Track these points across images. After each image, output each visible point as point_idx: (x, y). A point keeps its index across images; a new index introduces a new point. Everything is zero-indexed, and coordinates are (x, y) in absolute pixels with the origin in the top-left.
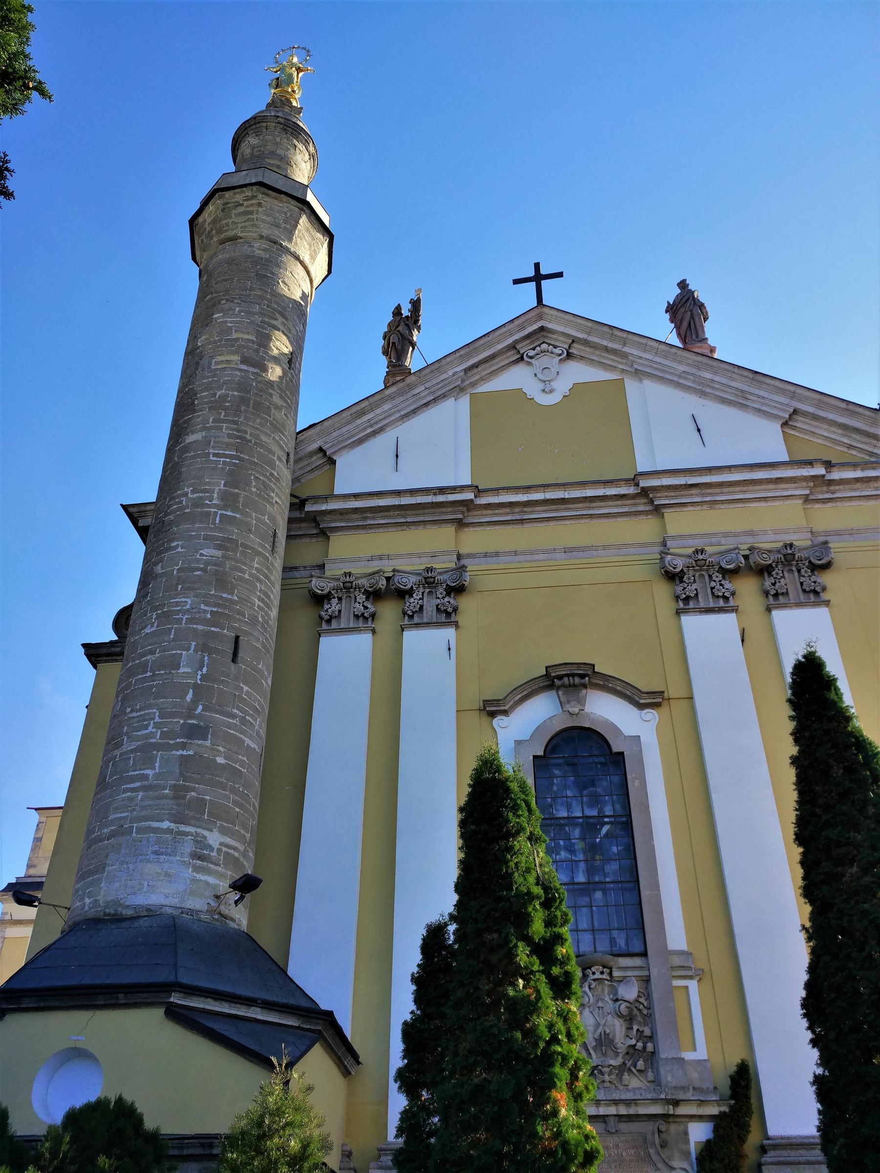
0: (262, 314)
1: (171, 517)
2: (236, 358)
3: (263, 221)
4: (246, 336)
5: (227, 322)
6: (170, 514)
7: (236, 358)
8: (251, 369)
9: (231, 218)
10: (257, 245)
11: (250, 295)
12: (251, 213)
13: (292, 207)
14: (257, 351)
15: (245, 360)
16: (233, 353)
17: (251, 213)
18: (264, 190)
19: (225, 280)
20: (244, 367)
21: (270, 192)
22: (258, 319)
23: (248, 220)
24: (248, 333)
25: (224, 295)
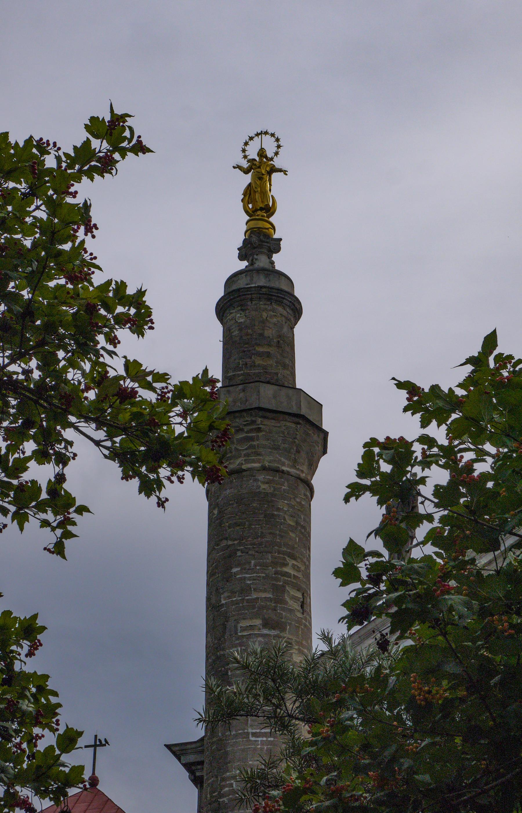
0: (274, 564)
1: (225, 799)
2: (258, 622)
3: (264, 447)
4: (263, 595)
5: (245, 578)
6: (223, 796)
7: (258, 622)
8: (273, 632)
9: (233, 443)
10: (261, 477)
11: (260, 544)
12: (252, 439)
13: (288, 424)
14: (275, 609)
15: (266, 624)
16: (255, 616)
17: (252, 439)
18: (261, 413)
19: (237, 524)
20: (265, 631)
21: (268, 414)
22: (271, 570)
23: (251, 447)
24: (265, 591)
25: (240, 544)
